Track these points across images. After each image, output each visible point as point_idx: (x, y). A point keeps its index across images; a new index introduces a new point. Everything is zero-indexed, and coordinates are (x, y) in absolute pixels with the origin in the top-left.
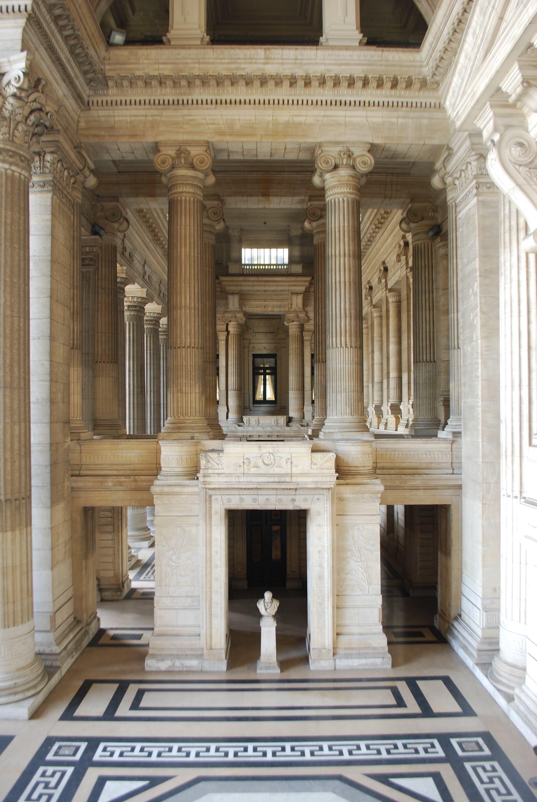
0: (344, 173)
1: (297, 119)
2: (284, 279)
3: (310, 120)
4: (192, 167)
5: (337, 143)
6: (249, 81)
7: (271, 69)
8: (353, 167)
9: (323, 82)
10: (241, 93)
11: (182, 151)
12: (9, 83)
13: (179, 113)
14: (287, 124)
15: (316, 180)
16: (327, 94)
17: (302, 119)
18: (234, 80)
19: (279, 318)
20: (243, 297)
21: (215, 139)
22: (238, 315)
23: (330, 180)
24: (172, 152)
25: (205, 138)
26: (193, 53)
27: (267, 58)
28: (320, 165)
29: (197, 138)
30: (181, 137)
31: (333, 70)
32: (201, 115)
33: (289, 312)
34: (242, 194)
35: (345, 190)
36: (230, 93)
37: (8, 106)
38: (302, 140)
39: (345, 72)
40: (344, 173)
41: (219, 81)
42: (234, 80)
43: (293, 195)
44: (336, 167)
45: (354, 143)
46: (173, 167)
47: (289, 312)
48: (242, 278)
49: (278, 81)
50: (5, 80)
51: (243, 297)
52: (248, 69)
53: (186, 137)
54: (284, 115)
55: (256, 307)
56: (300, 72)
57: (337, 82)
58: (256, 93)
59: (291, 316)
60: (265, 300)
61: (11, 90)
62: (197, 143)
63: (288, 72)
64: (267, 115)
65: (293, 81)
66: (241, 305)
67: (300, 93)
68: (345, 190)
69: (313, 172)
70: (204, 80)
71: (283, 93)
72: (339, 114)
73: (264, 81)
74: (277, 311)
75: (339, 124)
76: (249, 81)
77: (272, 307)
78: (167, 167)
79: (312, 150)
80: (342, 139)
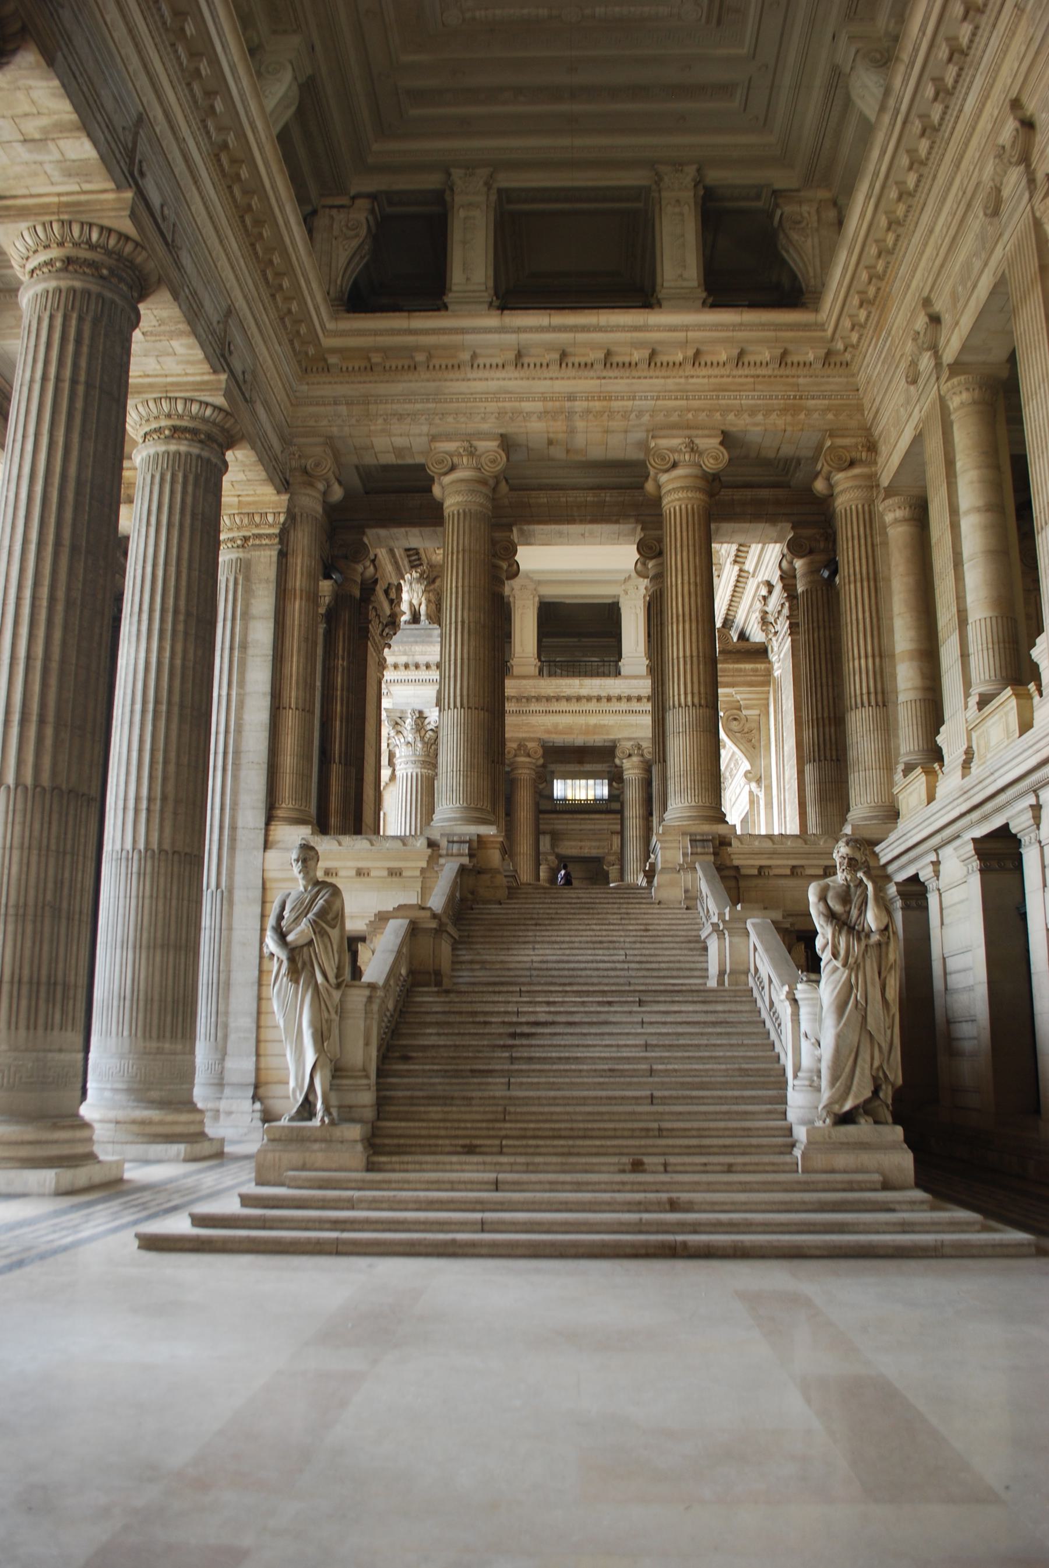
0: (635, 759)
1: (602, 722)
2: (603, 816)
3: (611, 723)
4: (529, 756)
5: (630, 739)
6: (568, 699)
7: (584, 692)
8: (642, 755)
9: (619, 698)
10: (563, 706)
11: (521, 745)
12: (429, 723)
13: (520, 718)
14: (595, 726)
15: (617, 761)
16: (623, 706)
17: (606, 722)
18: (558, 699)
19: (598, 860)
20: (556, 837)
21: (545, 736)
22: (550, 858)
23: (627, 764)
24: (514, 745)
25: (538, 735)
26: (531, 682)
27: (581, 685)
28: (618, 753)
29: (532, 735)
30: (521, 735)
31: (626, 692)
32: (534, 720)
33: (608, 854)
34: (561, 762)
35: (637, 771)
36: (555, 706)
37: (427, 735)
38: (606, 737)
39: (635, 693)
40: (635, 759)
41: (548, 699)
42: (558, 699)
43: (603, 762)
44: (630, 755)
45: (642, 739)
46: (515, 756)
47: (608, 854)
48: (554, 816)
49: (589, 699)
50: (427, 721)
51: (556, 837)
52: (568, 692)
53: (524, 735)
54: (593, 720)
55: (570, 848)
56: (603, 694)
57: (629, 699)
58: (574, 706)
59: (612, 858)
60: (581, 840)
61: (429, 727)
62: (532, 740)
63: (595, 694)
64: (581, 720)
65: (599, 699)
66: (553, 846)
67: (604, 706)
68: (637, 771)
69: (614, 757)
70: (538, 699)
71: (592, 706)
72: (632, 719)
73: (579, 699)
74: (594, 852)
75: (632, 725)
76: (568, 699)
77: (589, 849)
78: (511, 756)
79: (614, 741)
80: (634, 736)
